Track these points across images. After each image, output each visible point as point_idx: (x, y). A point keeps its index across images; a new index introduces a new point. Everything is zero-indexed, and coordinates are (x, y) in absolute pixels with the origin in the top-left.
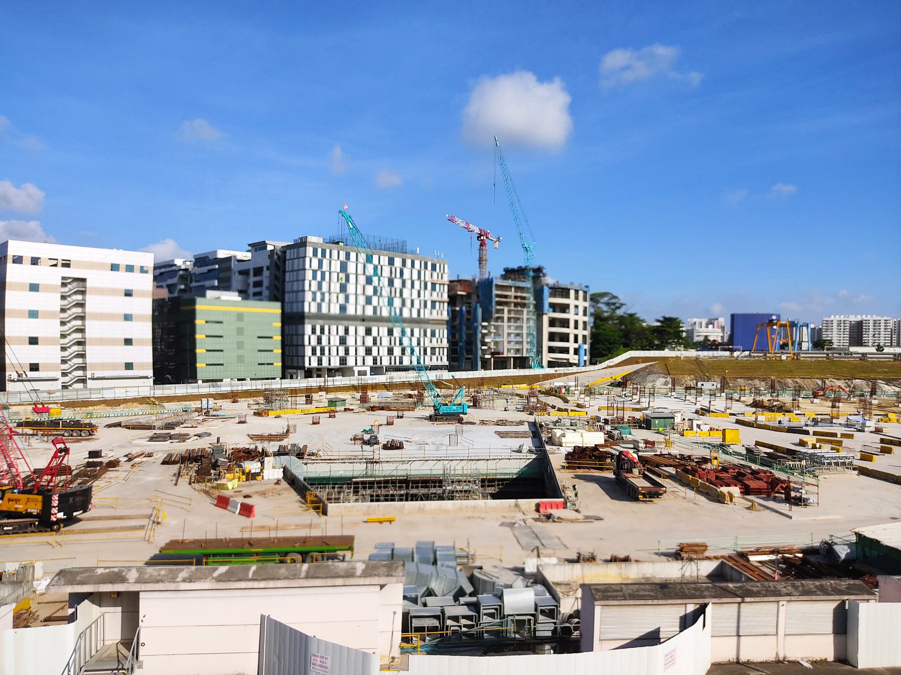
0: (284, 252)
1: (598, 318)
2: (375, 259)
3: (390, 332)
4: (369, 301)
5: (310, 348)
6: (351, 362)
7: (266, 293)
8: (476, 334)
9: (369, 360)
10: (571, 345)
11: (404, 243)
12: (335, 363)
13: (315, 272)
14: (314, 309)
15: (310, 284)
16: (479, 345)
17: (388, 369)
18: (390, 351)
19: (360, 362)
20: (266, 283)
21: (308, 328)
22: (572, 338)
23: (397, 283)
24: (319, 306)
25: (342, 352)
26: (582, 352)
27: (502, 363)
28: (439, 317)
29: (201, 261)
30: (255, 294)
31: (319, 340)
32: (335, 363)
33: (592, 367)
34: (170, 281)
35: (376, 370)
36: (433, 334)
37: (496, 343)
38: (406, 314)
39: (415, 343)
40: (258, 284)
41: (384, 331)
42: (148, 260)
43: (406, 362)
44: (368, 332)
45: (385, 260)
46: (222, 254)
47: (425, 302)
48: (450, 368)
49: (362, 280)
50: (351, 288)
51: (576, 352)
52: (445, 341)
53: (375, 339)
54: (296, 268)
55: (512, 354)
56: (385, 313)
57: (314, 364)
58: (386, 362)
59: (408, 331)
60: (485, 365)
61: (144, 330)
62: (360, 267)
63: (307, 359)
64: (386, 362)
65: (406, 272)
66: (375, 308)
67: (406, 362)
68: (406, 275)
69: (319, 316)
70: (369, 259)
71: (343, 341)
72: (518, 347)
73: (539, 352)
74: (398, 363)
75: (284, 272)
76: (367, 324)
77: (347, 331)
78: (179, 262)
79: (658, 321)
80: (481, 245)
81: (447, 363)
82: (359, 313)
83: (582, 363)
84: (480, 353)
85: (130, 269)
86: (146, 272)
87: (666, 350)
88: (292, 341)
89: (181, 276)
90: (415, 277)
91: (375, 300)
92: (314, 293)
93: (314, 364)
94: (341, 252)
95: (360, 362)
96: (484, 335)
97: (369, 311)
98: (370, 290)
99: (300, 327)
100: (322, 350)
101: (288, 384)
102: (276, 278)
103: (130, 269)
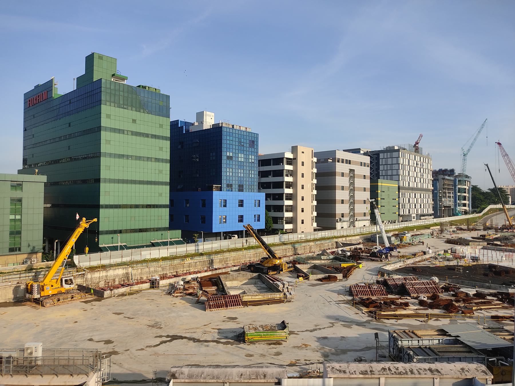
8: (437, 197)
10: (466, 202)
13: (402, 165)
21: (401, 193)
48: (436, 215)
51: (469, 205)
71: (409, 202)
81: (433, 212)
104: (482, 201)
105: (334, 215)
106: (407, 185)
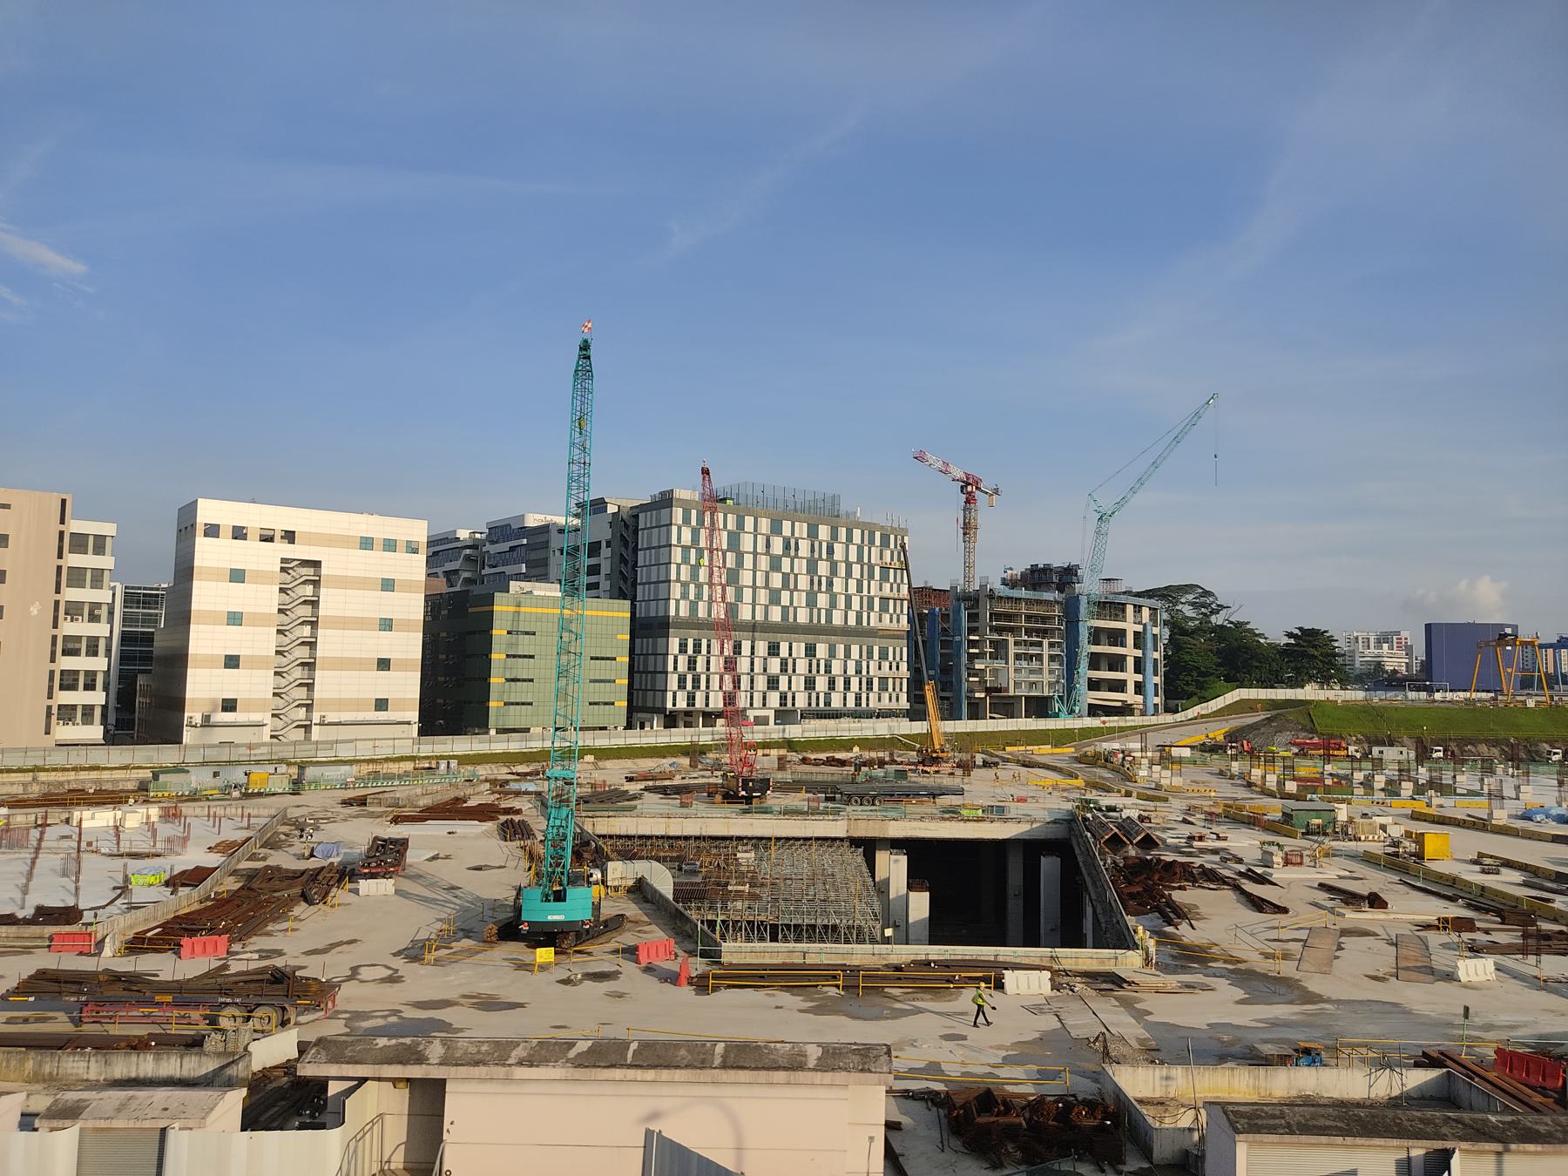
0: (636, 517)
1: (1177, 628)
2: (787, 525)
3: (810, 651)
4: (775, 598)
5: (676, 677)
6: (742, 701)
7: (605, 585)
8: (959, 656)
9: (774, 699)
10: (1130, 676)
11: (835, 499)
12: (717, 702)
14: (684, 612)
15: (679, 571)
16: (965, 674)
17: (808, 714)
18: (810, 684)
19: (757, 702)
20: (605, 568)
21: (674, 644)
22: (1130, 663)
23: (823, 568)
24: (693, 607)
25: (728, 686)
26: (1150, 689)
27: (1006, 707)
28: (894, 625)
29: (499, 532)
30: (590, 587)
31: (692, 663)
32: (717, 702)
33: (1169, 718)
34: (450, 566)
35: (785, 715)
36: (883, 655)
37: (995, 672)
38: (837, 620)
39: (851, 670)
40: (594, 570)
41: (799, 649)
42: (418, 531)
43: (836, 702)
44: (773, 650)
45: (802, 529)
46: (533, 521)
47: (871, 600)
49: (764, 562)
50: (746, 578)
51: (1139, 688)
52: (904, 666)
53: (784, 663)
54: (655, 544)
55: (1023, 692)
56: (803, 617)
57: (682, 704)
58: (801, 702)
59: (841, 649)
61: (409, 646)
62: (761, 540)
63: (670, 695)
64: (801, 702)
65: (839, 550)
66: (785, 610)
67: (836, 702)
68: (839, 554)
69: (692, 623)
70: (776, 529)
71: (730, 665)
72: (1033, 678)
73: (1070, 687)
74: (822, 705)
75: (636, 550)
76: (773, 637)
77: (737, 648)
78: (463, 534)
79: (1290, 635)
80: (968, 501)
82: (759, 617)
83: (1151, 710)
84: (965, 686)
85: (390, 545)
86: (415, 551)
87: (1308, 687)
88: (646, 665)
89: (467, 558)
90: (853, 557)
91: (785, 597)
92: (685, 585)
93: (682, 704)
94: (730, 516)
95: (757, 702)
96: (972, 657)
97: (776, 615)
98: (776, 580)
99: (661, 641)
100: (696, 680)
101: (635, 738)
102: (623, 560)
103: (390, 545)
104: (1201, 674)
105: (178, 704)
106: (719, 612)
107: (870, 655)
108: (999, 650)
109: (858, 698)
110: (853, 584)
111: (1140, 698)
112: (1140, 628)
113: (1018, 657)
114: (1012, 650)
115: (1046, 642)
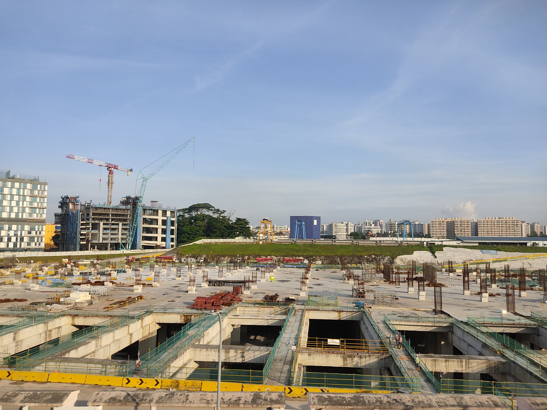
36: (32, 229)
47: (24, 208)
51: (164, 239)
55: (109, 241)
60: (83, 248)
107: (23, 229)
108: (95, 226)
109: (15, 244)
110: (14, 203)
111: (164, 243)
112: (165, 218)
113: (105, 229)
114: (102, 226)
115: (120, 224)
